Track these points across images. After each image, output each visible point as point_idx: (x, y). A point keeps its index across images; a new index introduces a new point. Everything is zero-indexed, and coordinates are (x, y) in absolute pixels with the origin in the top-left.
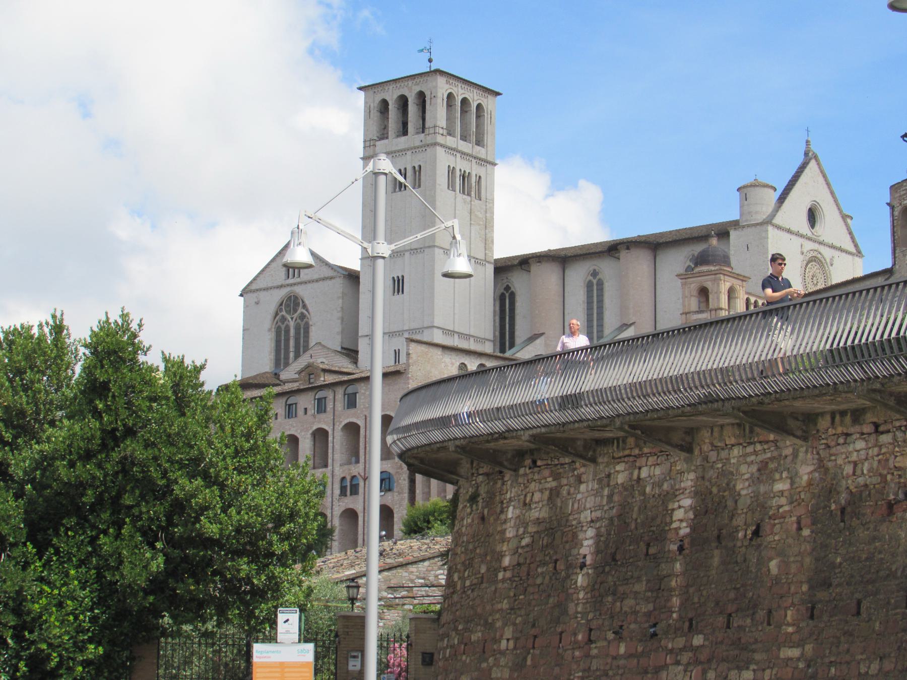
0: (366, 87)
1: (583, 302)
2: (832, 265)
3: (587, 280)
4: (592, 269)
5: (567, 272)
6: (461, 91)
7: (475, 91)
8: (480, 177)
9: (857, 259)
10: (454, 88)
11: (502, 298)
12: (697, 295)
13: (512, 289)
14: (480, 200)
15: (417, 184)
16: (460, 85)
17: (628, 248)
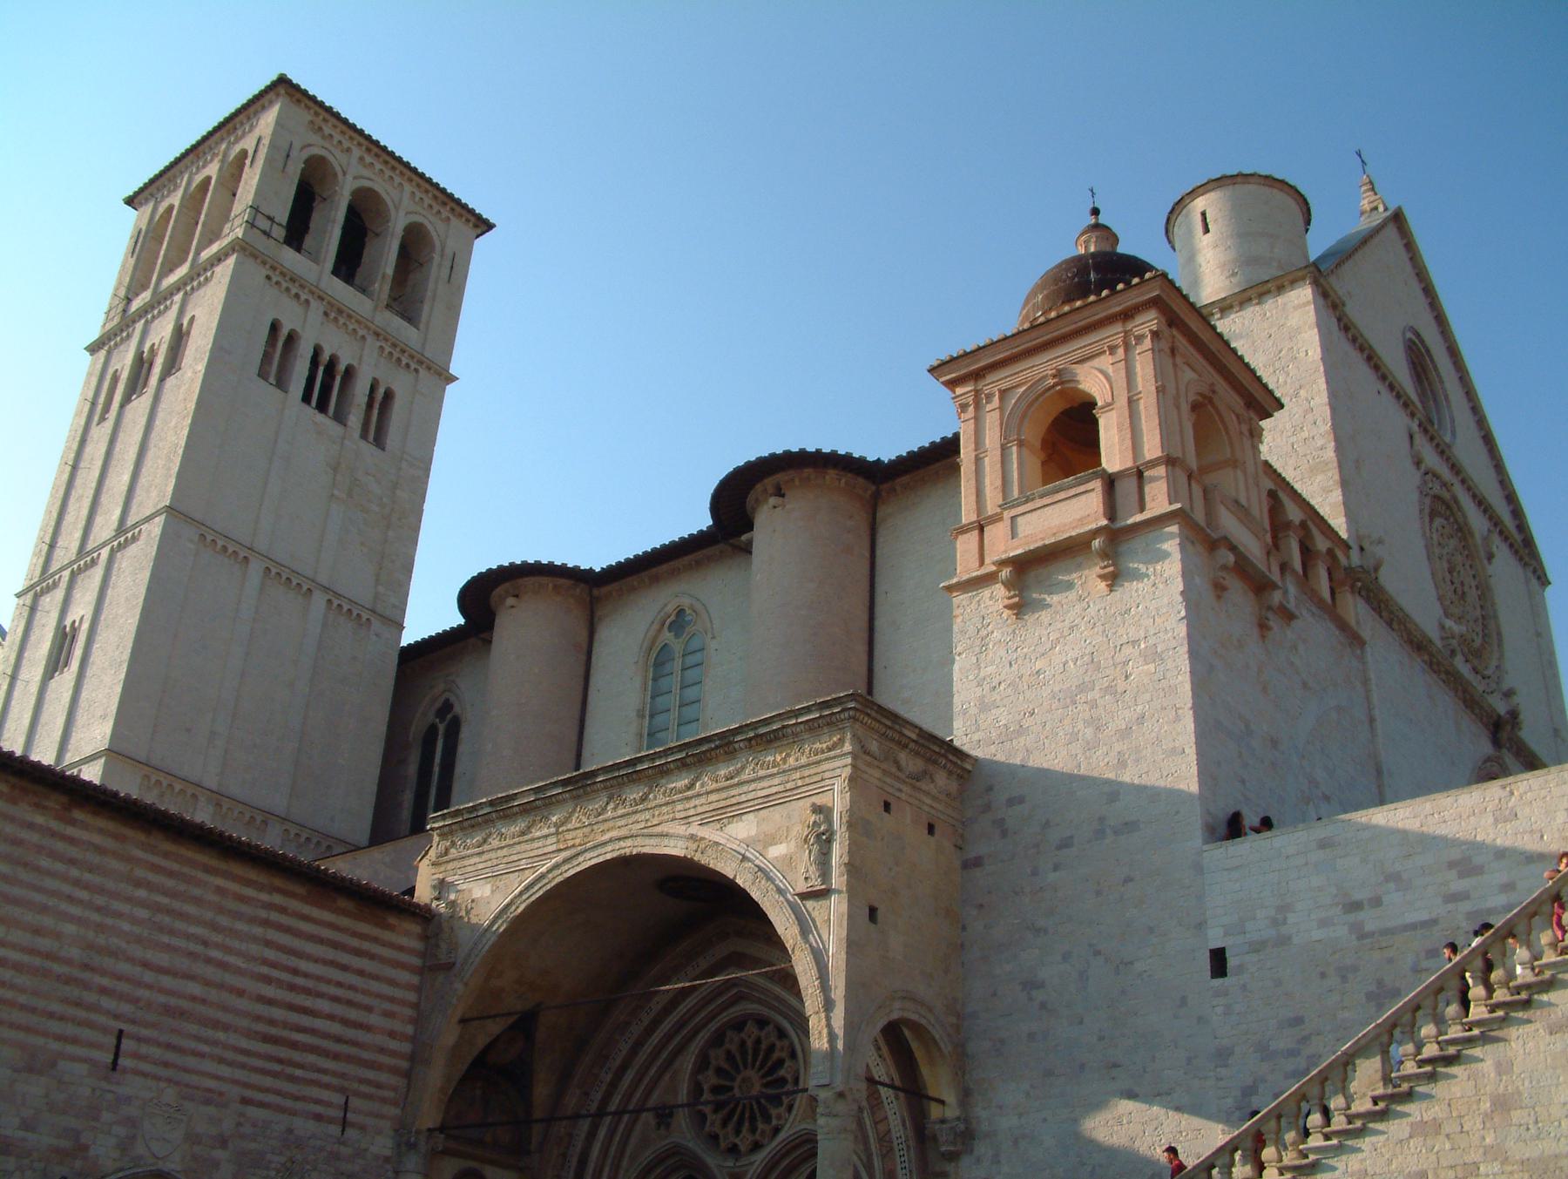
0: (137, 194)
1: (641, 715)
2: (1490, 557)
3: (659, 645)
4: (670, 608)
5: (597, 637)
6: (355, 169)
7: (408, 188)
8: (389, 396)
9: (1534, 581)
10: (337, 153)
11: (431, 732)
12: (1038, 444)
13: (457, 709)
14: (379, 441)
15: (172, 365)
16: (357, 152)
17: (779, 493)
